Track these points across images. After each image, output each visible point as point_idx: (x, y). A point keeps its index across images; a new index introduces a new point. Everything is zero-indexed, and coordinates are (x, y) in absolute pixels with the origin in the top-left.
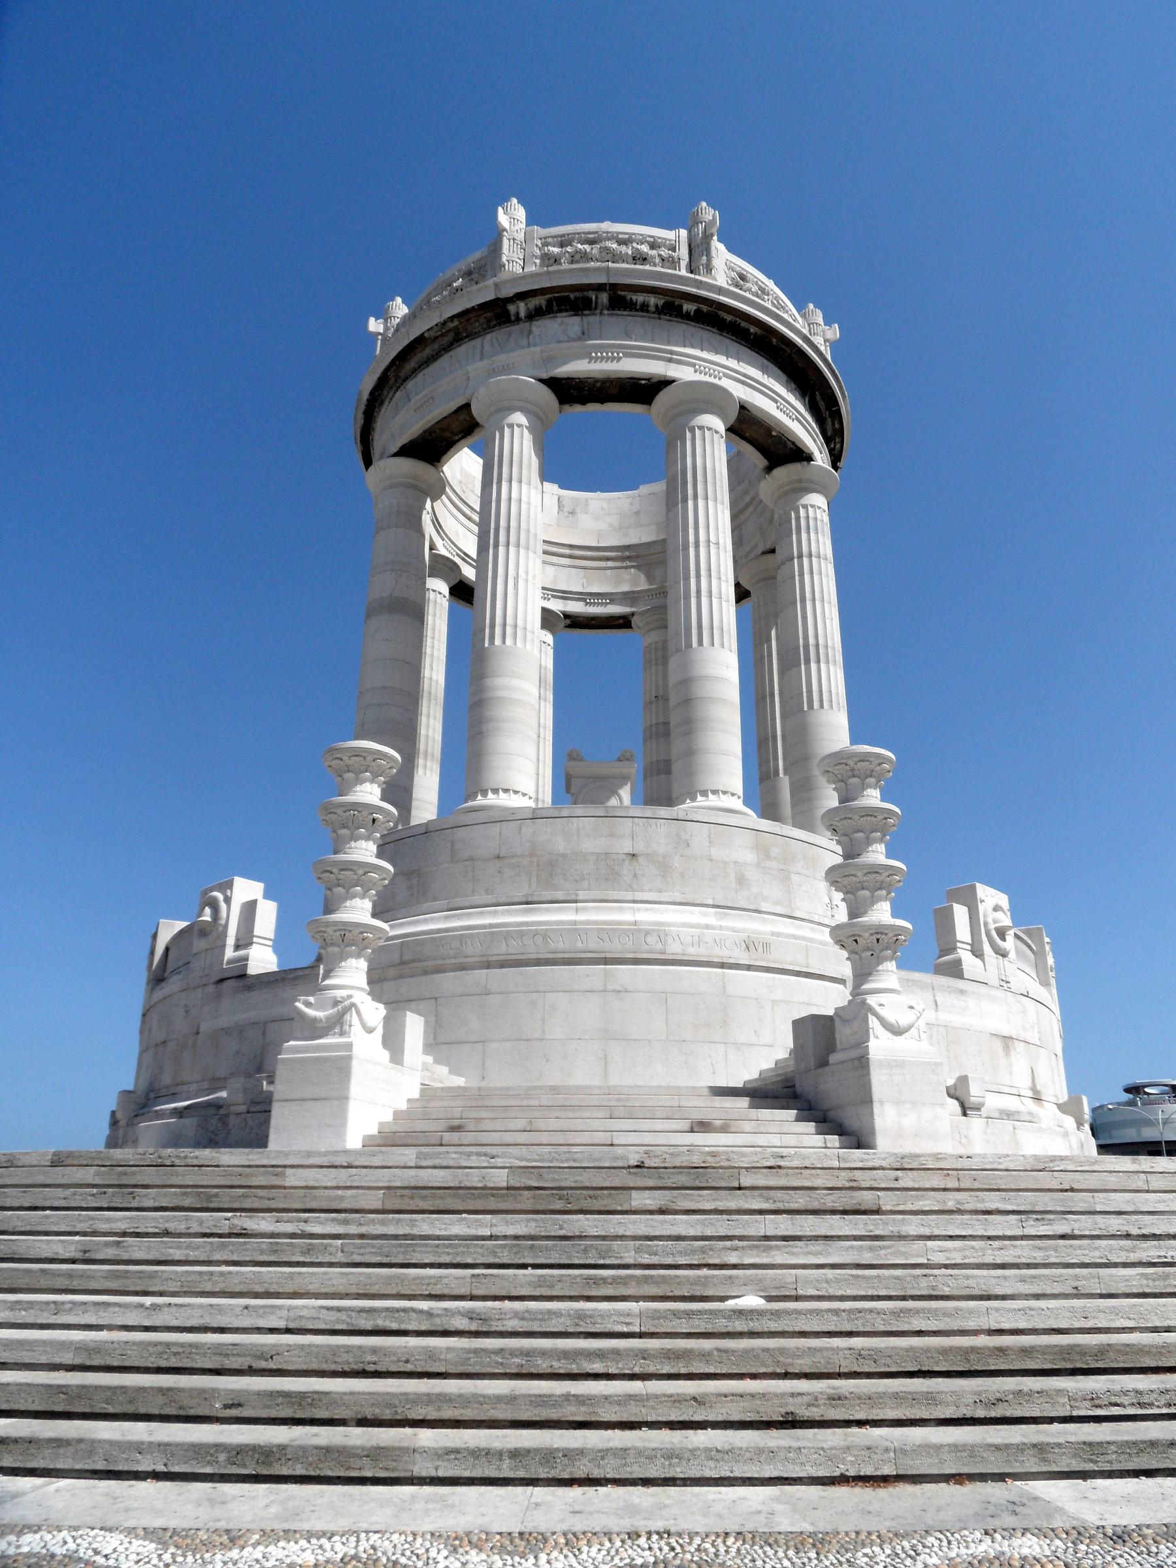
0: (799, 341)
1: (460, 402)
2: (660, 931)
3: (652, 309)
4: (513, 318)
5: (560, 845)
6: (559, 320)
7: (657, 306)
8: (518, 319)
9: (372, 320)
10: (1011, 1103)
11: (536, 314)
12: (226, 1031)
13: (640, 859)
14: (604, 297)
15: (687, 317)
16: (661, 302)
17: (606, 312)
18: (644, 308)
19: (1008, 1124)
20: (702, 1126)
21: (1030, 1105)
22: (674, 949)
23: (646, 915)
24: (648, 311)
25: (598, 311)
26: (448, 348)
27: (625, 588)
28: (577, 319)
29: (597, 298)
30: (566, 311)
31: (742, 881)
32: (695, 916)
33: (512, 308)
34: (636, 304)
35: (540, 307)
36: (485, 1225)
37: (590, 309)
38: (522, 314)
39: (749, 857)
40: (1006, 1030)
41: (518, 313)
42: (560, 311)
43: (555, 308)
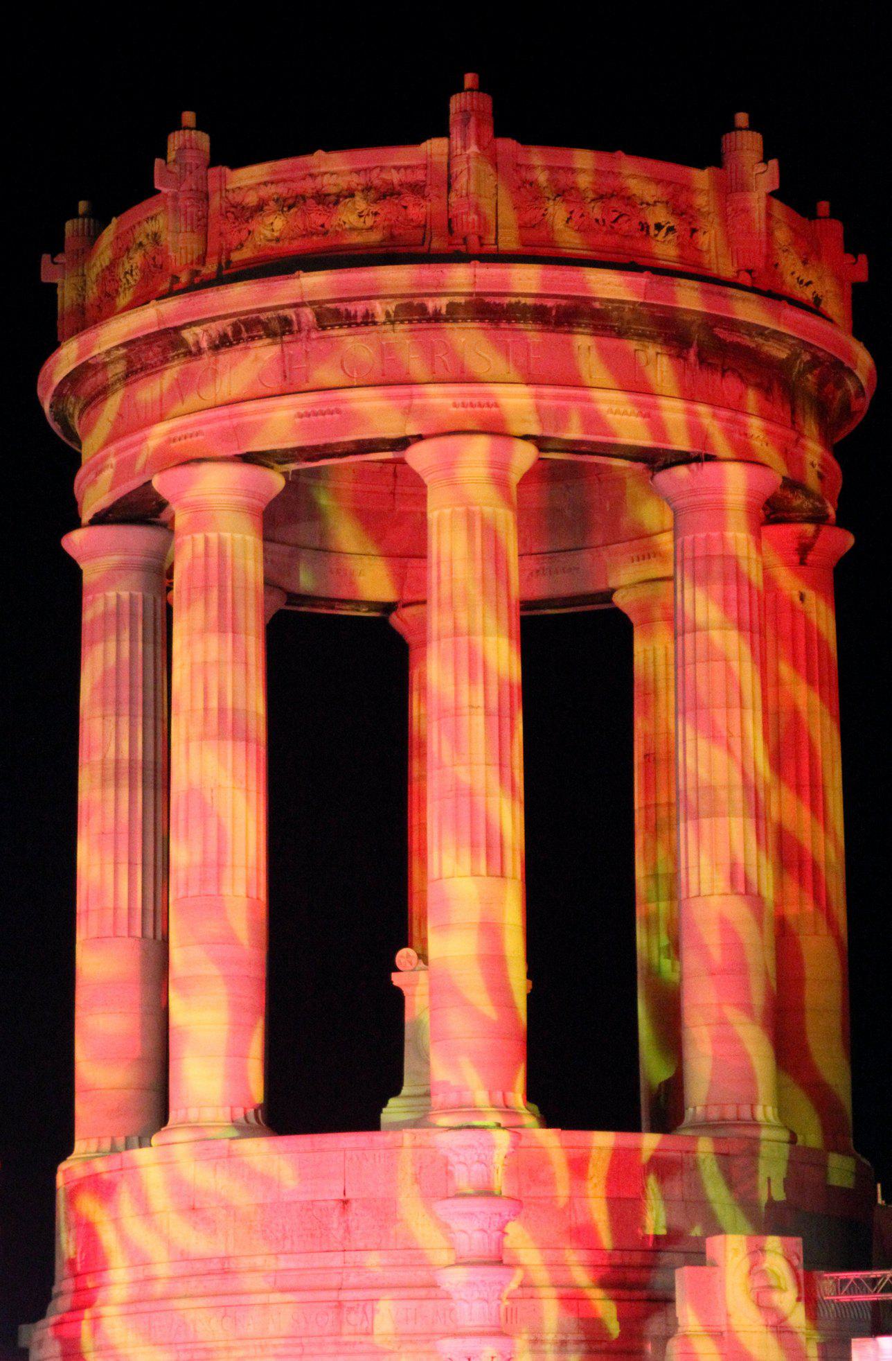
1: (146, 480)
3: (381, 318)
4: (193, 349)
6: (252, 353)
7: (388, 314)
8: (200, 351)
9: (46, 258)
11: (222, 343)
13: (354, 1205)
14: (308, 314)
16: (391, 308)
17: (314, 335)
24: (375, 323)
25: (304, 334)
29: (298, 315)
30: (260, 337)
33: (187, 335)
34: (355, 316)
35: (226, 335)
37: (291, 332)
38: (204, 345)
41: (197, 343)
42: (253, 338)
43: (245, 335)
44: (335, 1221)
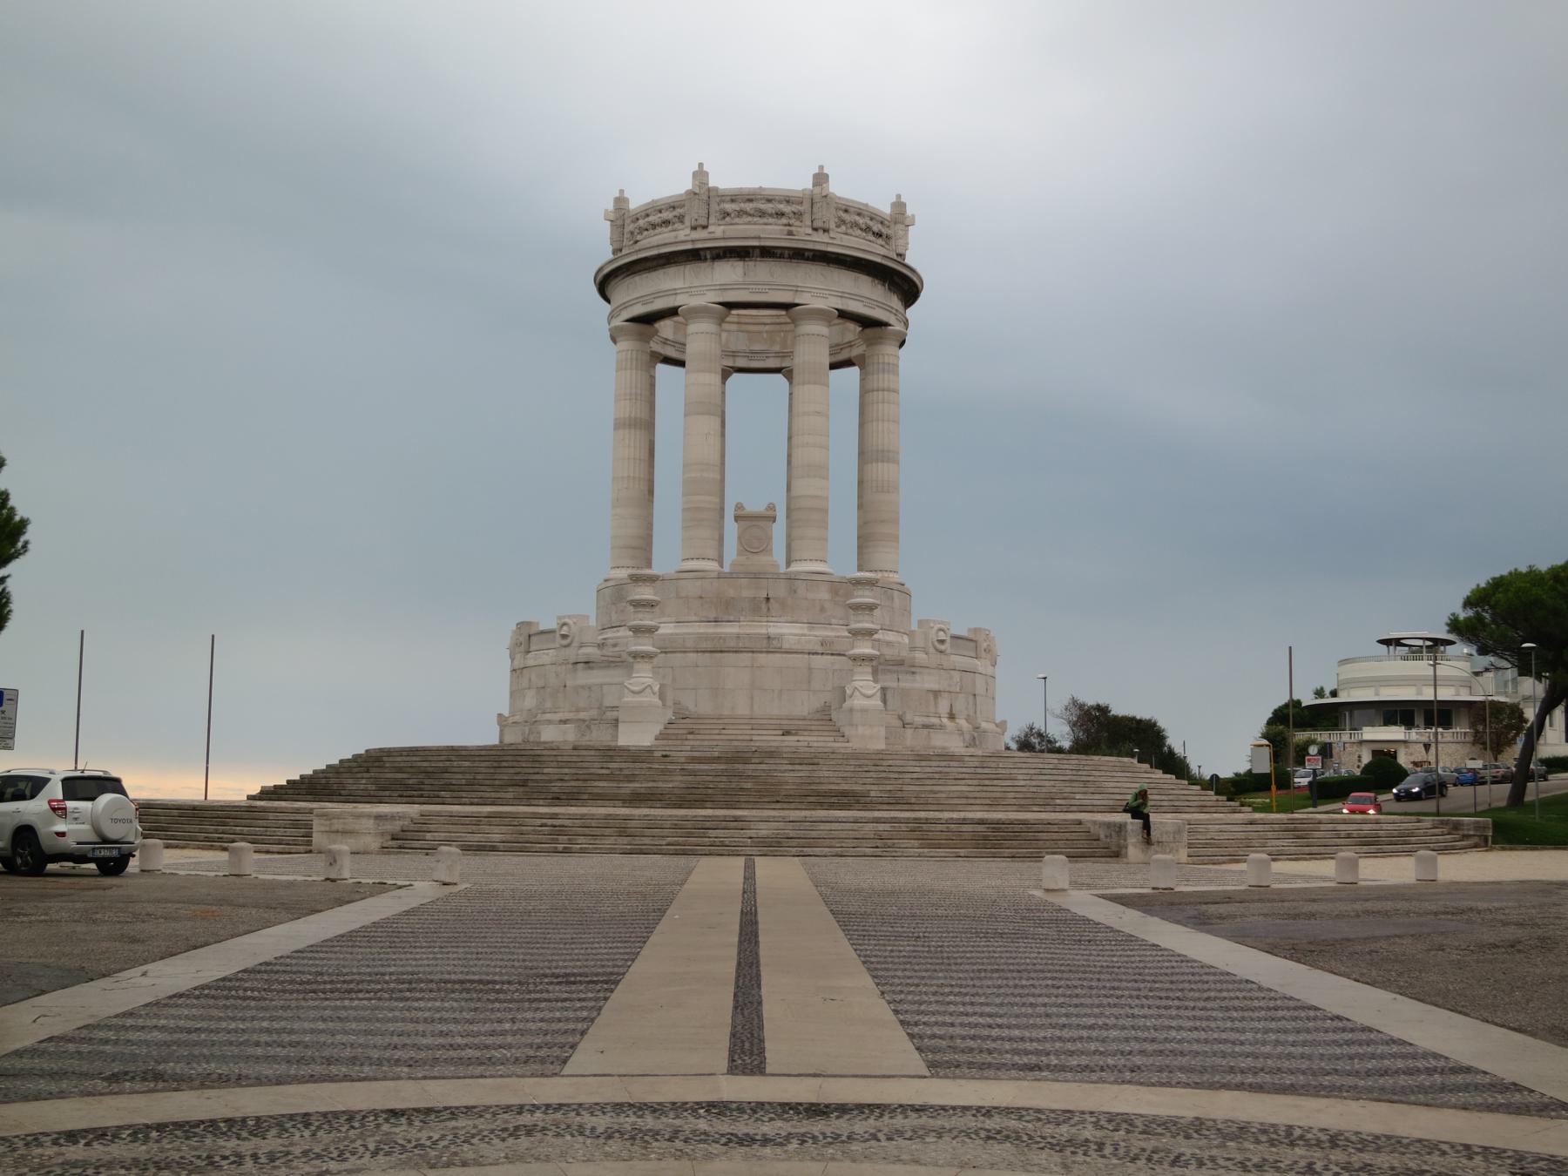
0: (878, 260)
2: (779, 637)
5: (731, 593)
10: (935, 721)
12: (583, 687)
15: (808, 259)
18: (781, 256)
19: (925, 731)
20: (787, 733)
21: (945, 721)
22: (786, 646)
23: (774, 629)
26: (663, 266)
27: (777, 348)
28: (741, 263)
31: (822, 609)
32: (796, 629)
36: (714, 766)
39: (827, 596)
40: (936, 687)
44: (764, 606)
